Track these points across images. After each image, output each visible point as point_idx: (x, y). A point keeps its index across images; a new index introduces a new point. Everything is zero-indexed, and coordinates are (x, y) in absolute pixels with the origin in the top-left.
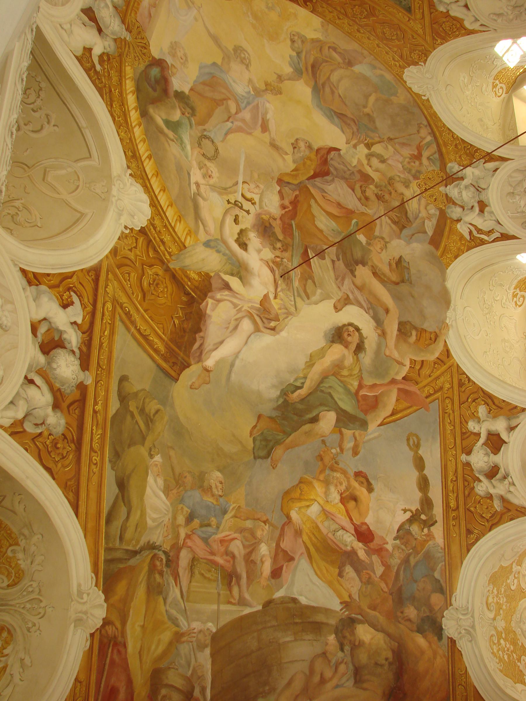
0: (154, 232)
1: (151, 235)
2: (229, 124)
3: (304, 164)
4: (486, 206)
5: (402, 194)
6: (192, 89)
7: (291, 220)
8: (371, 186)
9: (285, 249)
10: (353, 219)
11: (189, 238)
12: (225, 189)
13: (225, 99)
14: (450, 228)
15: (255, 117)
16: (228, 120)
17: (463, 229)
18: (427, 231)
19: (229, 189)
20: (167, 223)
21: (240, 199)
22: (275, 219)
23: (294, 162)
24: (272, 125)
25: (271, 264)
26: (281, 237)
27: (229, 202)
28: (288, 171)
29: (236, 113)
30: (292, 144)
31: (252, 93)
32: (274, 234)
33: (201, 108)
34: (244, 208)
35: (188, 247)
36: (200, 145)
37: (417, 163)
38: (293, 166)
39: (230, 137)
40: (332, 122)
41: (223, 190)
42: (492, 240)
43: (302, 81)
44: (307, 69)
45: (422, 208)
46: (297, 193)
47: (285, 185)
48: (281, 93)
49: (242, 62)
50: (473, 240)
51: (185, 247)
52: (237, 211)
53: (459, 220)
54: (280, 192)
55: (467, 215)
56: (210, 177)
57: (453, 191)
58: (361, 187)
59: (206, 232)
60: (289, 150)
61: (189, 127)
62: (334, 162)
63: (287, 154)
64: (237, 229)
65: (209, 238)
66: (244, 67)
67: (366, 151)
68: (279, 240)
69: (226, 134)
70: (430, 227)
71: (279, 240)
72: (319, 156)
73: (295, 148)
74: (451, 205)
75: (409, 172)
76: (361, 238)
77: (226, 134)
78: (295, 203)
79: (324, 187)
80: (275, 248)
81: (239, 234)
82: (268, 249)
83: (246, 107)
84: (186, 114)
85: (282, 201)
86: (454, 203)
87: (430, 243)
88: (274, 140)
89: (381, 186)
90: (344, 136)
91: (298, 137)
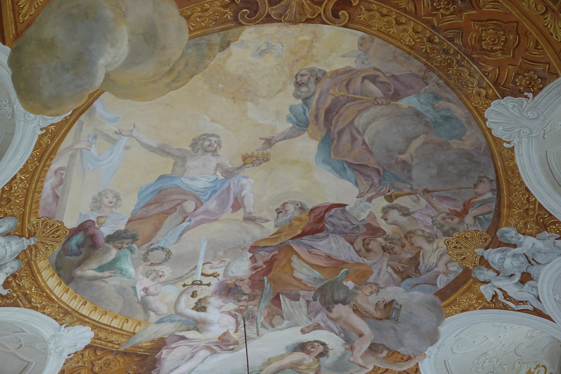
44: (316, 117)
79: (313, 244)
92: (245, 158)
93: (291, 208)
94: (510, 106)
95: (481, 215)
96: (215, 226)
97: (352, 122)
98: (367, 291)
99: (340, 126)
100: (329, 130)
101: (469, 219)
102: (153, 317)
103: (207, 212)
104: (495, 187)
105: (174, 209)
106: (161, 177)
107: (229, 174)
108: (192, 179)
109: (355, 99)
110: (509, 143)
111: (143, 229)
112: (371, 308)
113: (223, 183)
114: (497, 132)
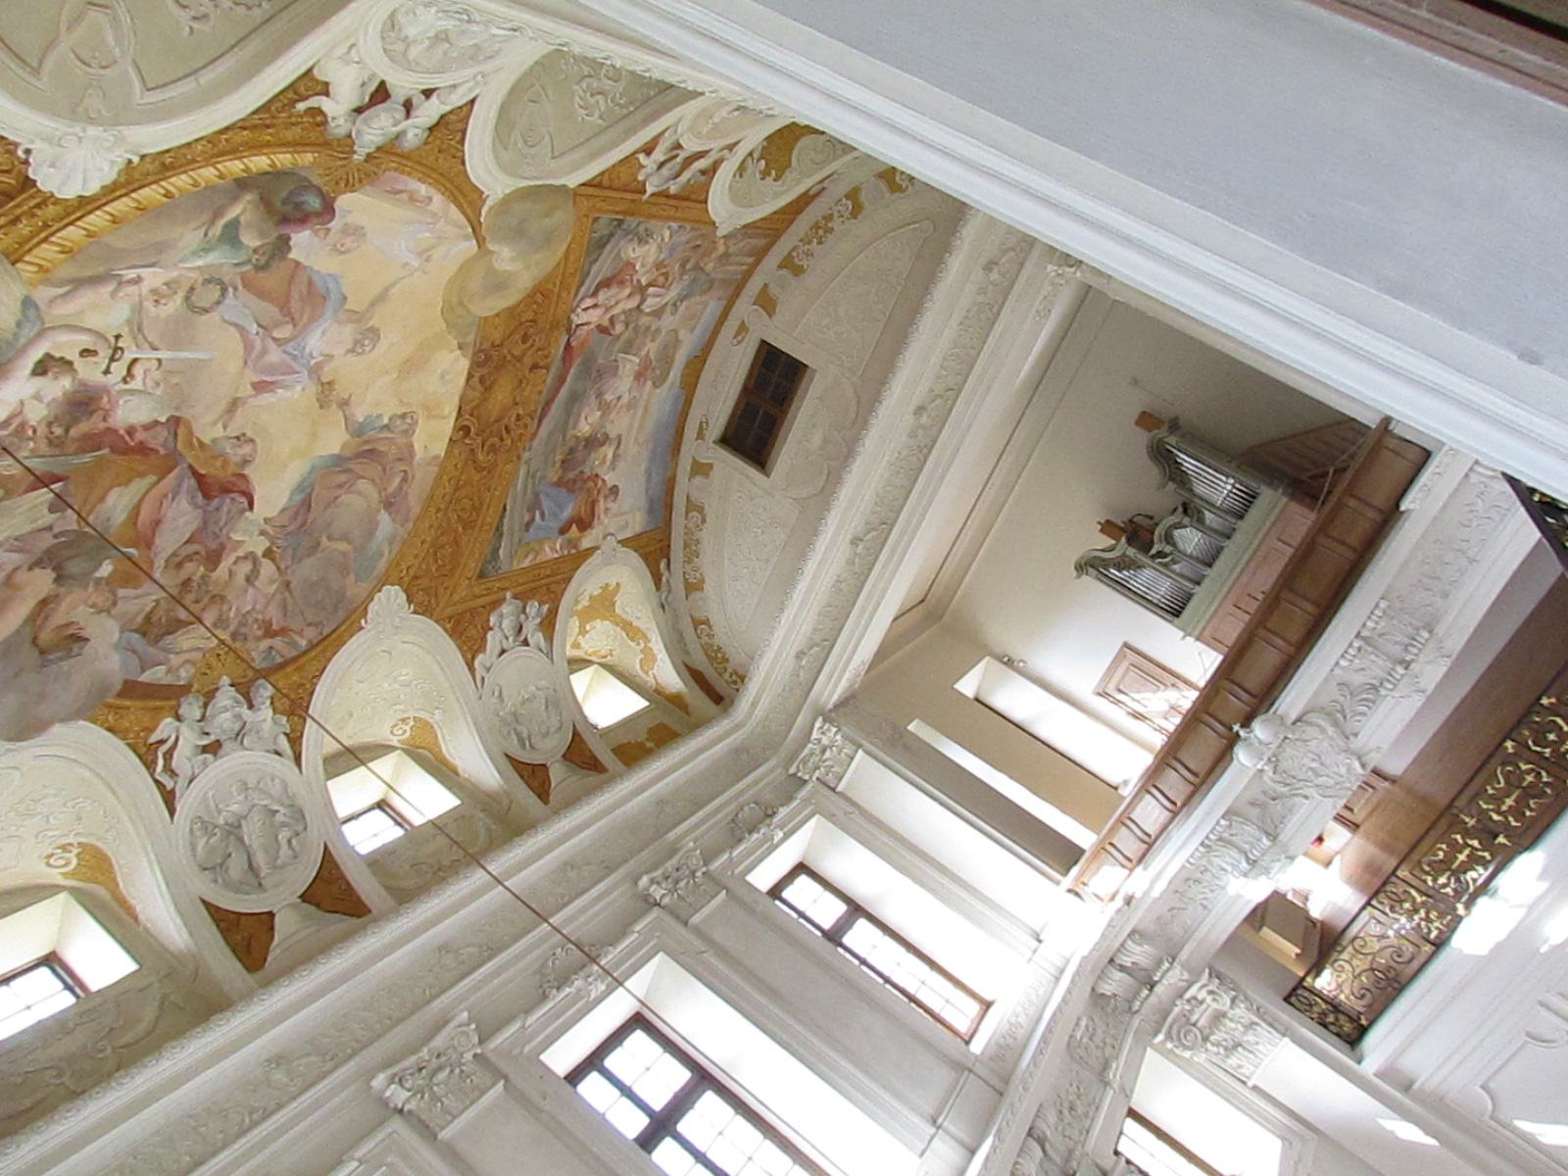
0: (32, 203)
1: (25, 199)
2: (254, 328)
3: (215, 458)
4: (215, 754)
6: (297, 263)
7: (111, 447)
8: (202, 569)
9: (51, 442)
10: (137, 548)
11: (35, 269)
12: (140, 329)
13: (293, 319)
14: (161, 708)
15: (273, 369)
16: (259, 325)
17: (166, 727)
18: (147, 673)
19: (140, 337)
20: (54, 228)
21: (128, 356)
22: (105, 419)
23: (214, 441)
24: (267, 398)
25: (16, 422)
26: (73, 432)
27: (118, 337)
28: (197, 434)
29: (274, 339)
30: (244, 435)
31: (313, 362)
32: (76, 420)
33: (271, 280)
34: (114, 365)
35: (16, 269)
36: (208, 281)
37: (260, 633)
38: (206, 440)
39: (233, 329)
40: (292, 493)
41: (137, 327)
42: (159, 778)
46: (162, 451)
47: (172, 432)
48: (321, 407)
49: (356, 342)
50: (149, 749)
51: (13, 264)
52: (104, 354)
53: (179, 718)
54: (156, 423)
55: (192, 729)
56: (156, 301)
57: (226, 696)
58: (197, 553)
59: (52, 301)
60: (232, 431)
61: (235, 261)
62: (227, 504)
63: (225, 427)
64: (72, 355)
65: (42, 306)
66: (350, 346)
67: (259, 552)
68: (67, 431)
69: (236, 325)
70: (156, 675)
71: (67, 431)
72: (234, 479)
73: (238, 438)
74: (202, 700)
76: (106, 569)
77: (236, 325)
78: (143, 450)
80: (50, 424)
81: (62, 358)
82: (45, 412)
83: (289, 354)
84: (256, 256)
85: (140, 429)
86: (206, 706)
87: (126, 682)
88: (245, 403)
89: (206, 584)
90: (275, 514)
91: (258, 440)
94: (398, 601)
95: (277, 651)
97: (363, 477)
99: (358, 468)
100: (350, 459)
101: (265, 644)
104: (315, 642)
109: (384, 470)
110: (366, 622)
114: (373, 607)
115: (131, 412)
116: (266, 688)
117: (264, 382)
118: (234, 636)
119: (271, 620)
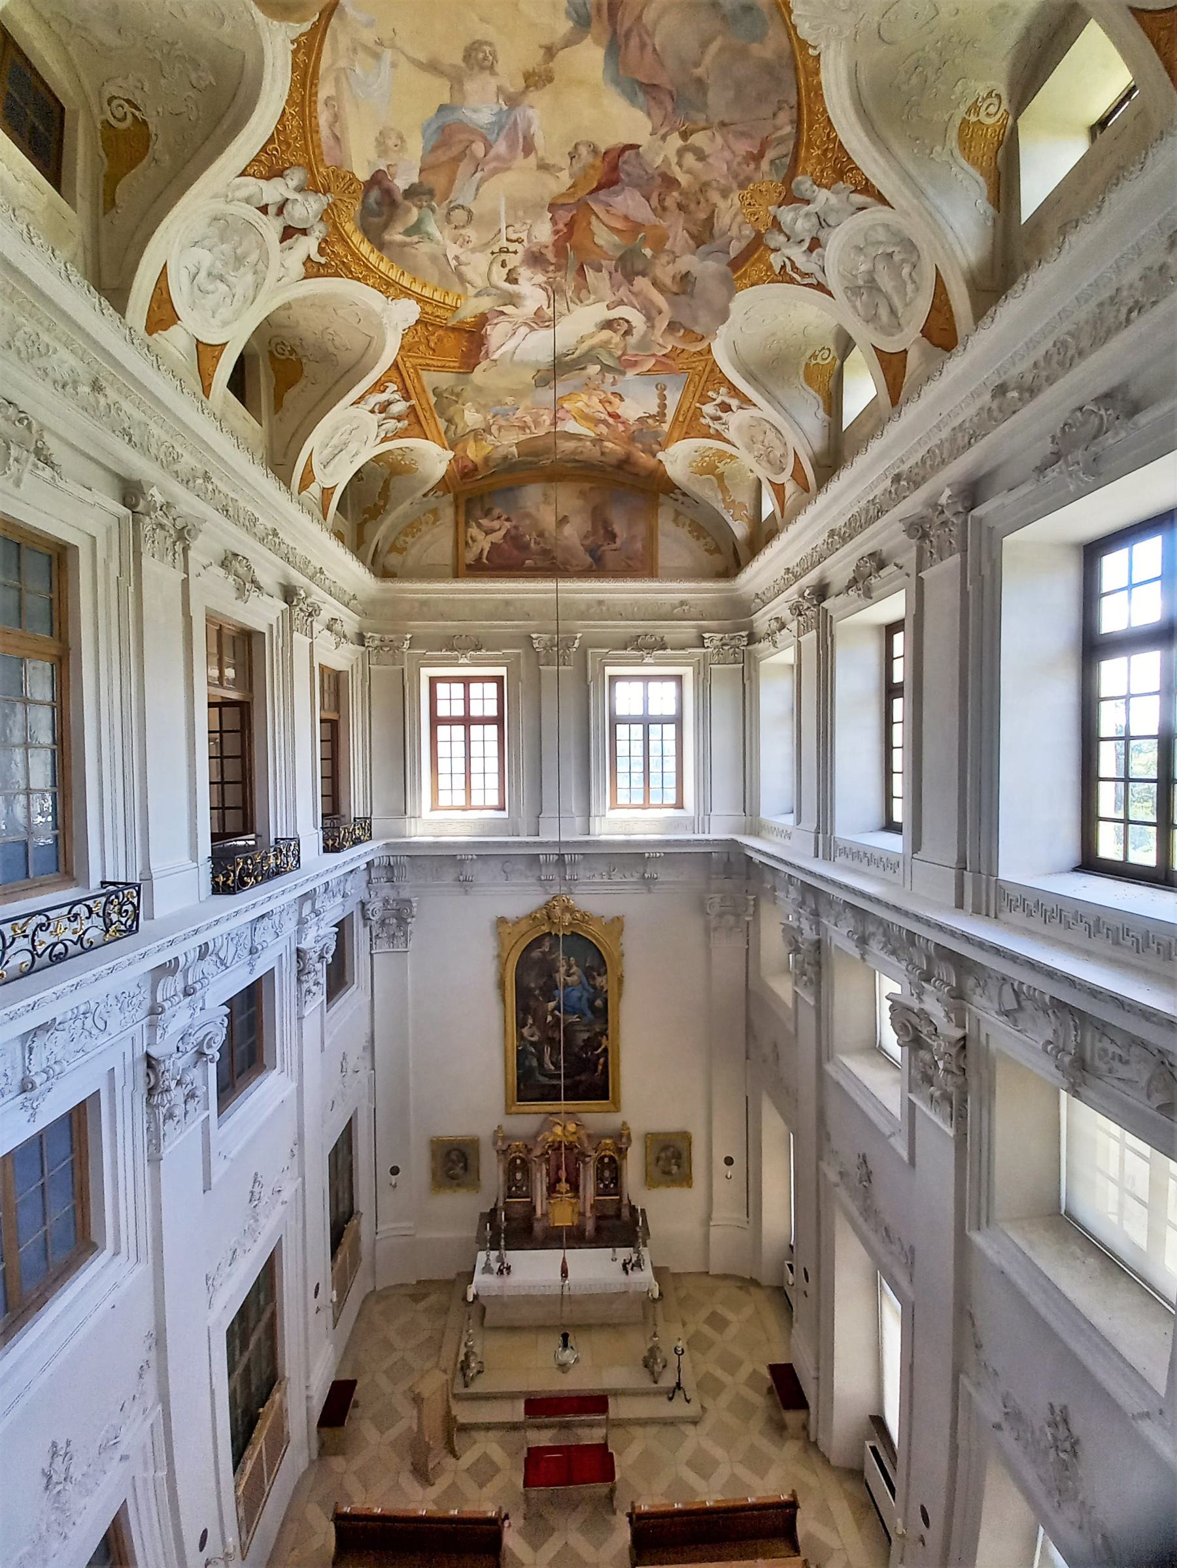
5: (715, 205)
43: (589, 40)
45: (735, 227)
75: (736, 177)
92: (528, 76)
93: (583, 150)
95: (778, 159)
96: (508, 178)
98: (664, 259)
101: (765, 165)
102: (471, 291)
103: (498, 158)
104: (795, 117)
105: (463, 154)
106: (442, 108)
107: (513, 101)
108: (475, 111)
110: (815, 48)
111: (438, 181)
112: (668, 281)
113: (508, 117)
115: (544, 232)
116: (800, 183)
117: (524, 146)
118: (742, 186)
119: (747, 152)
